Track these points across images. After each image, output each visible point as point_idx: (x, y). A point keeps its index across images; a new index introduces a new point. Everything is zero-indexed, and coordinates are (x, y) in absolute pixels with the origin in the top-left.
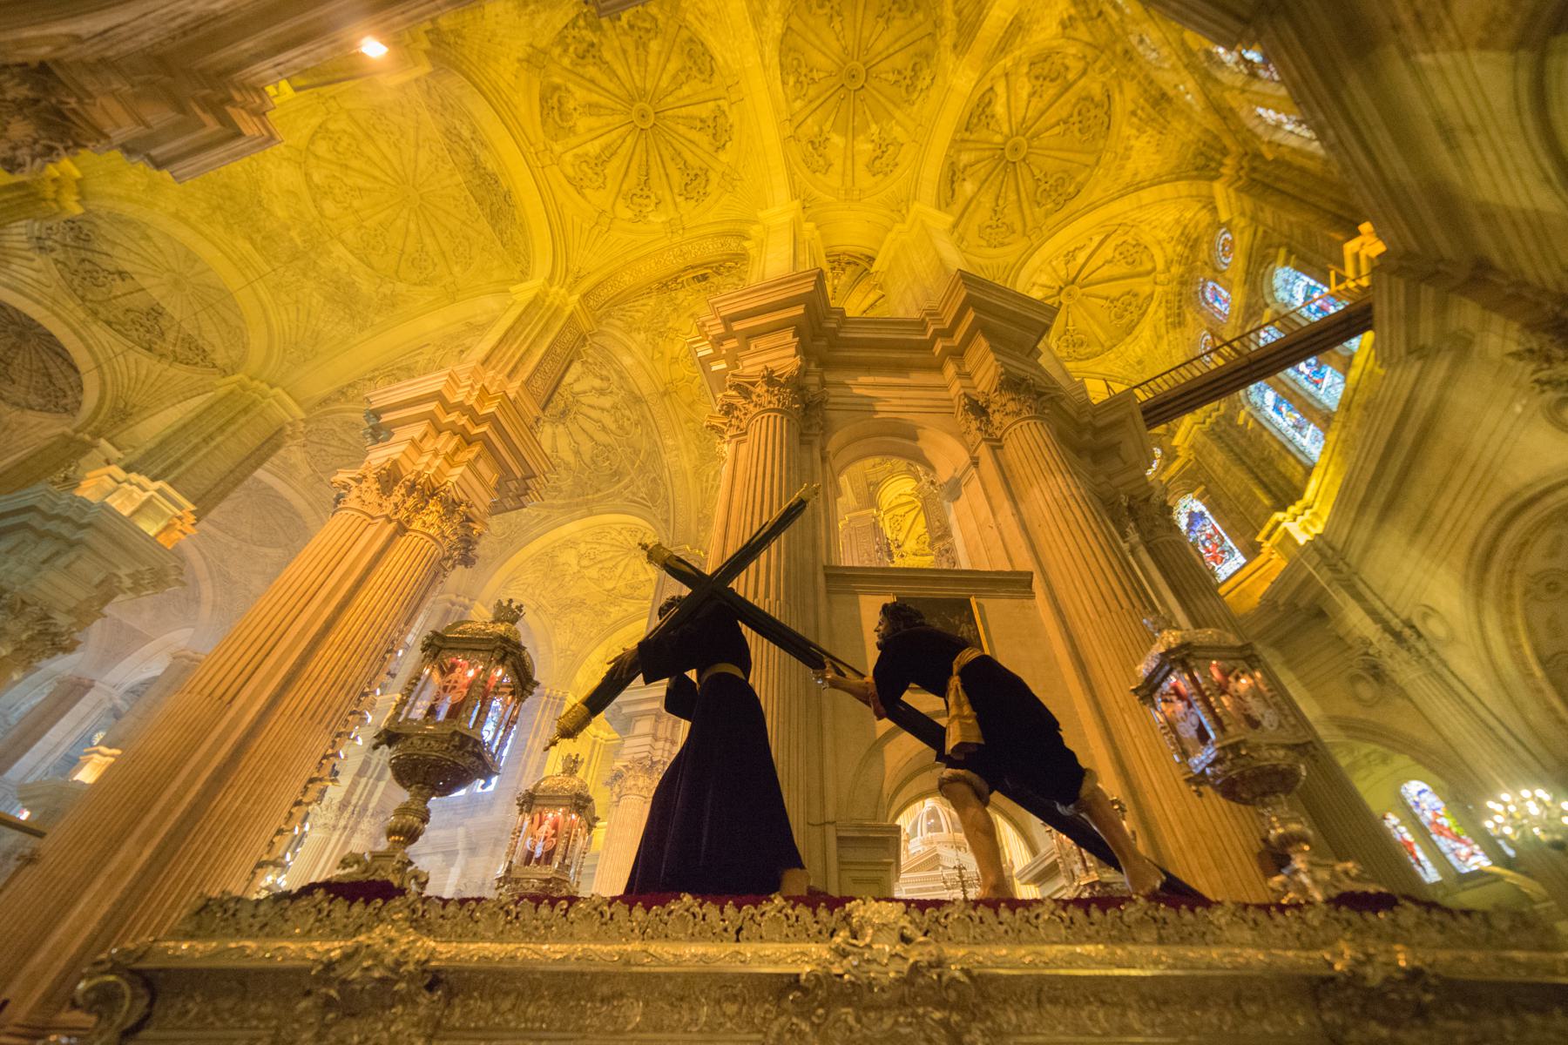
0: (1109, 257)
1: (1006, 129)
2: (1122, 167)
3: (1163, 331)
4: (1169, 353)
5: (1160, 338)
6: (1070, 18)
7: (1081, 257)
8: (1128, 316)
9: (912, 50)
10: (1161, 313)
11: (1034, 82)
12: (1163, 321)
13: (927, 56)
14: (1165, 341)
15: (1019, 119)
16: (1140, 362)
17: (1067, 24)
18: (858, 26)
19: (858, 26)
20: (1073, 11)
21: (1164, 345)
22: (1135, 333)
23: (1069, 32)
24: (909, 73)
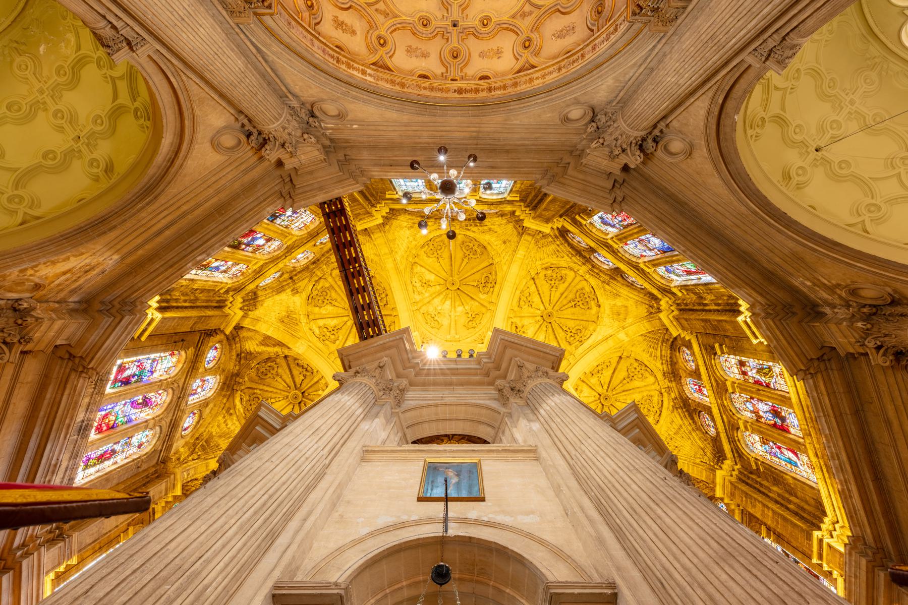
0: (435, 260)
1: (346, 319)
2: (372, 260)
3: (486, 228)
4: (499, 225)
5: (490, 229)
6: (292, 290)
7: (432, 277)
8: (475, 248)
9: (292, 366)
10: (475, 229)
11: (325, 303)
12: (480, 228)
13: (295, 359)
14: (492, 227)
15: (343, 311)
16: (505, 242)
17: (295, 291)
18: (275, 390)
19: (275, 390)
20: (289, 290)
21: (495, 228)
22: (485, 244)
23: (299, 291)
24: (301, 369)
